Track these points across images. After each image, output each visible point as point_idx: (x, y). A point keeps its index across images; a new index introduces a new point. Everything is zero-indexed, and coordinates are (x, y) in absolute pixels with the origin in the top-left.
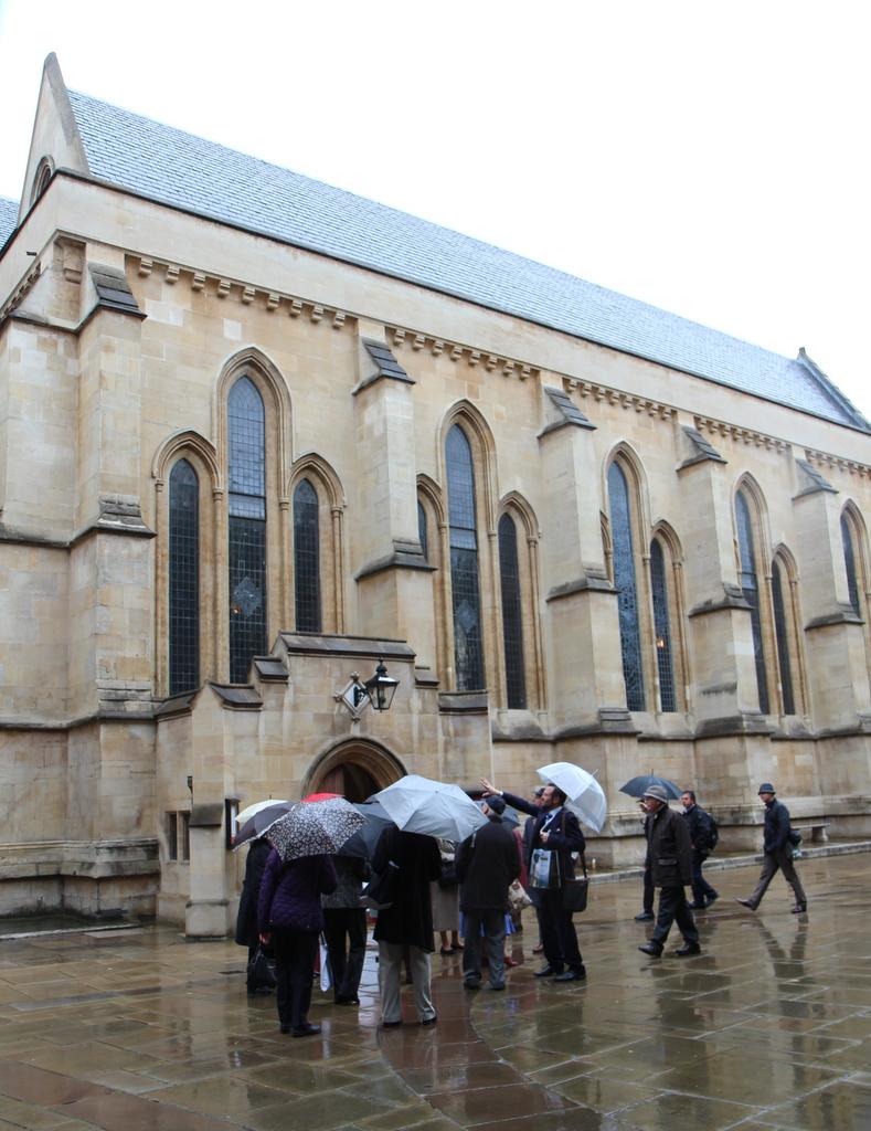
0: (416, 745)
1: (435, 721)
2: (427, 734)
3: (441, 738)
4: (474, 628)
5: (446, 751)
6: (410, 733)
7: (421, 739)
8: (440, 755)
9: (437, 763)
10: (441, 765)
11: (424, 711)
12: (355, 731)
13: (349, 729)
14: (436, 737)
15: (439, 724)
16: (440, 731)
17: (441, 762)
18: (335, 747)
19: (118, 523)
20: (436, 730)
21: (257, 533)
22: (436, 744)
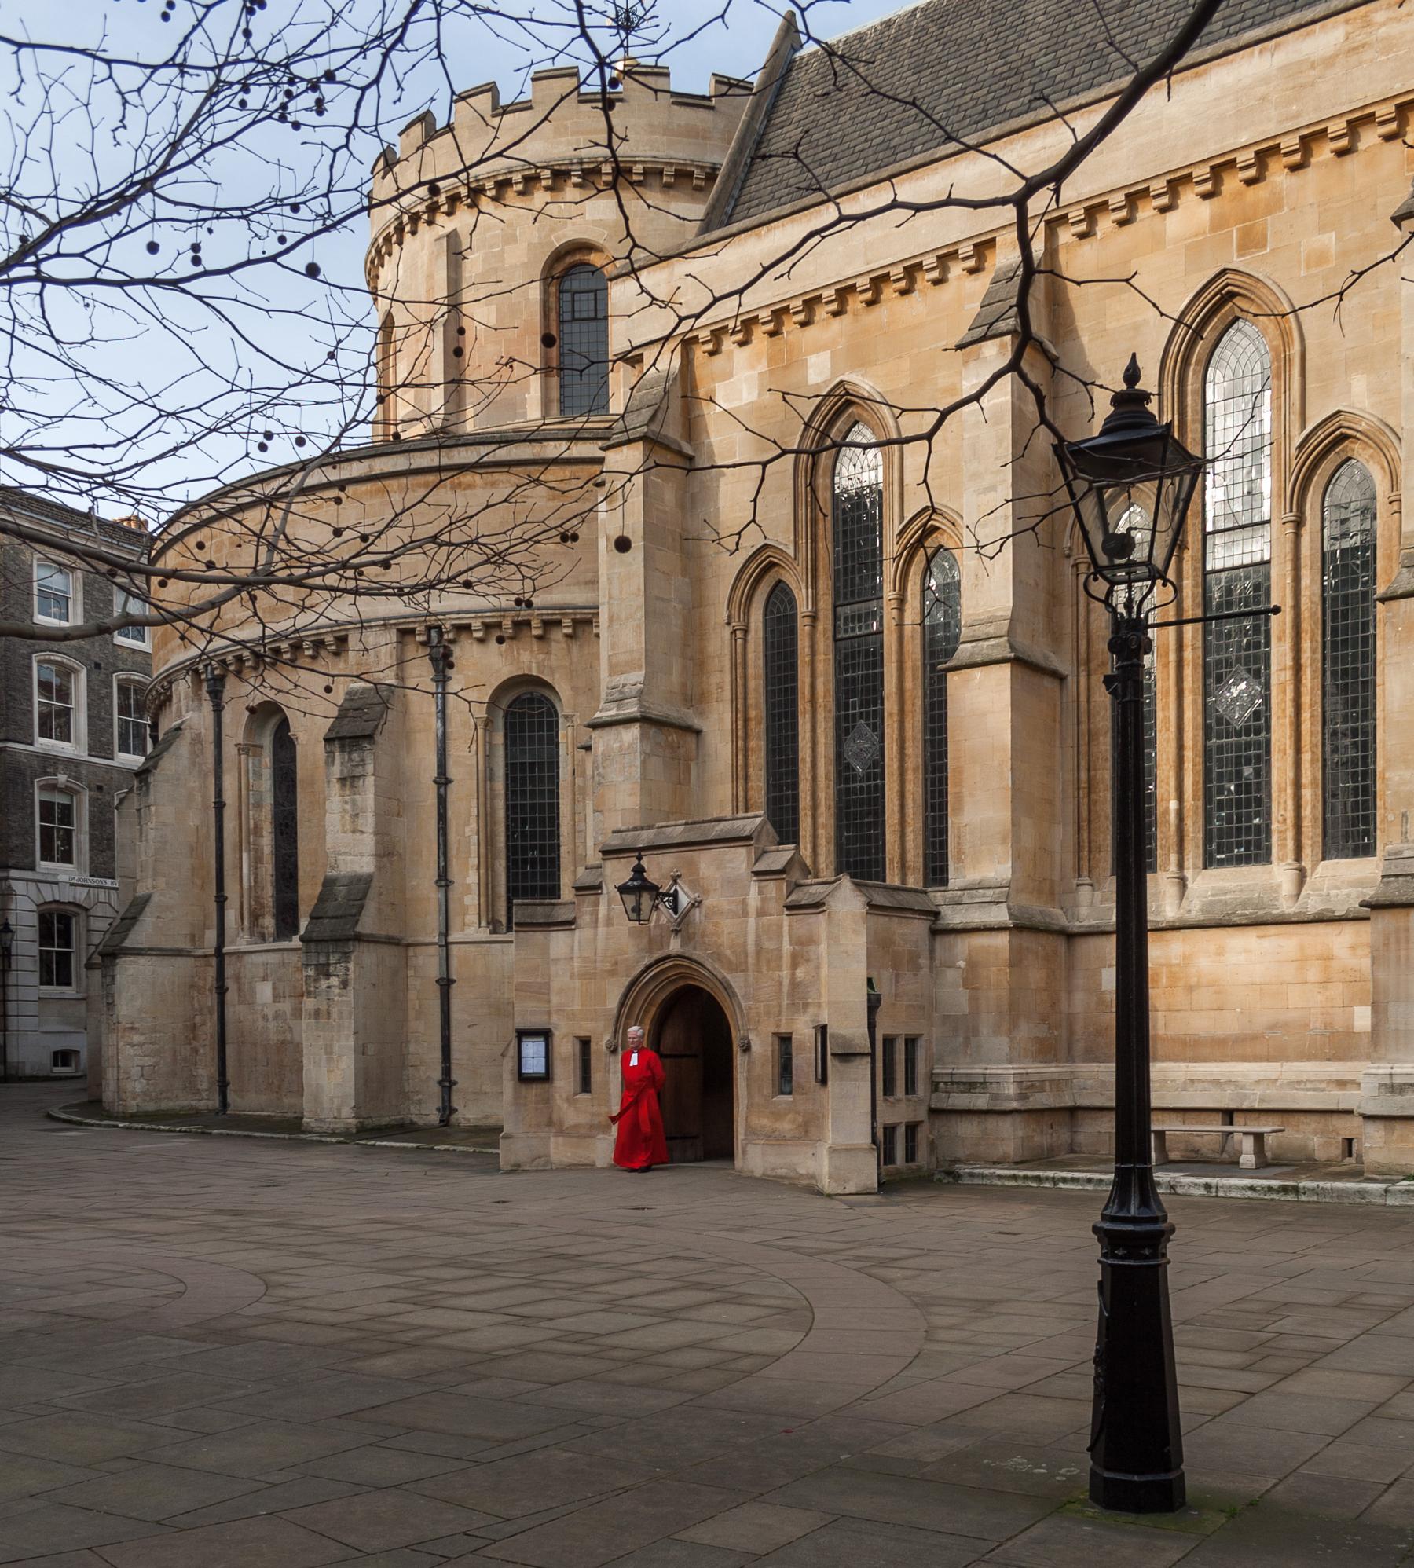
0: (751, 960)
1: (780, 927)
2: (768, 945)
3: (787, 948)
4: (1256, 715)
5: (794, 966)
6: (745, 945)
7: (759, 950)
8: (785, 973)
9: (781, 984)
10: (785, 989)
11: (761, 913)
12: (675, 946)
13: (668, 944)
14: (780, 949)
15: (786, 928)
16: (786, 939)
17: (786, 982)
18: (648, 968)
19: (614, 712)
20: (780, 936)
21: (874, 654)
22: (780, 957)
